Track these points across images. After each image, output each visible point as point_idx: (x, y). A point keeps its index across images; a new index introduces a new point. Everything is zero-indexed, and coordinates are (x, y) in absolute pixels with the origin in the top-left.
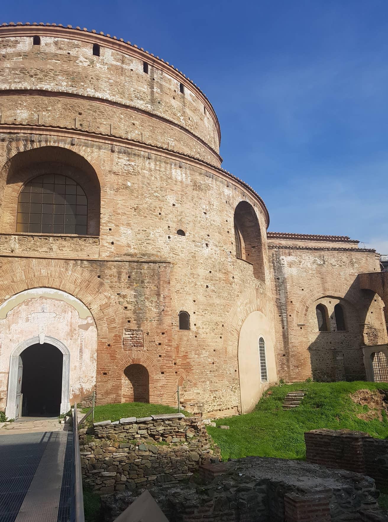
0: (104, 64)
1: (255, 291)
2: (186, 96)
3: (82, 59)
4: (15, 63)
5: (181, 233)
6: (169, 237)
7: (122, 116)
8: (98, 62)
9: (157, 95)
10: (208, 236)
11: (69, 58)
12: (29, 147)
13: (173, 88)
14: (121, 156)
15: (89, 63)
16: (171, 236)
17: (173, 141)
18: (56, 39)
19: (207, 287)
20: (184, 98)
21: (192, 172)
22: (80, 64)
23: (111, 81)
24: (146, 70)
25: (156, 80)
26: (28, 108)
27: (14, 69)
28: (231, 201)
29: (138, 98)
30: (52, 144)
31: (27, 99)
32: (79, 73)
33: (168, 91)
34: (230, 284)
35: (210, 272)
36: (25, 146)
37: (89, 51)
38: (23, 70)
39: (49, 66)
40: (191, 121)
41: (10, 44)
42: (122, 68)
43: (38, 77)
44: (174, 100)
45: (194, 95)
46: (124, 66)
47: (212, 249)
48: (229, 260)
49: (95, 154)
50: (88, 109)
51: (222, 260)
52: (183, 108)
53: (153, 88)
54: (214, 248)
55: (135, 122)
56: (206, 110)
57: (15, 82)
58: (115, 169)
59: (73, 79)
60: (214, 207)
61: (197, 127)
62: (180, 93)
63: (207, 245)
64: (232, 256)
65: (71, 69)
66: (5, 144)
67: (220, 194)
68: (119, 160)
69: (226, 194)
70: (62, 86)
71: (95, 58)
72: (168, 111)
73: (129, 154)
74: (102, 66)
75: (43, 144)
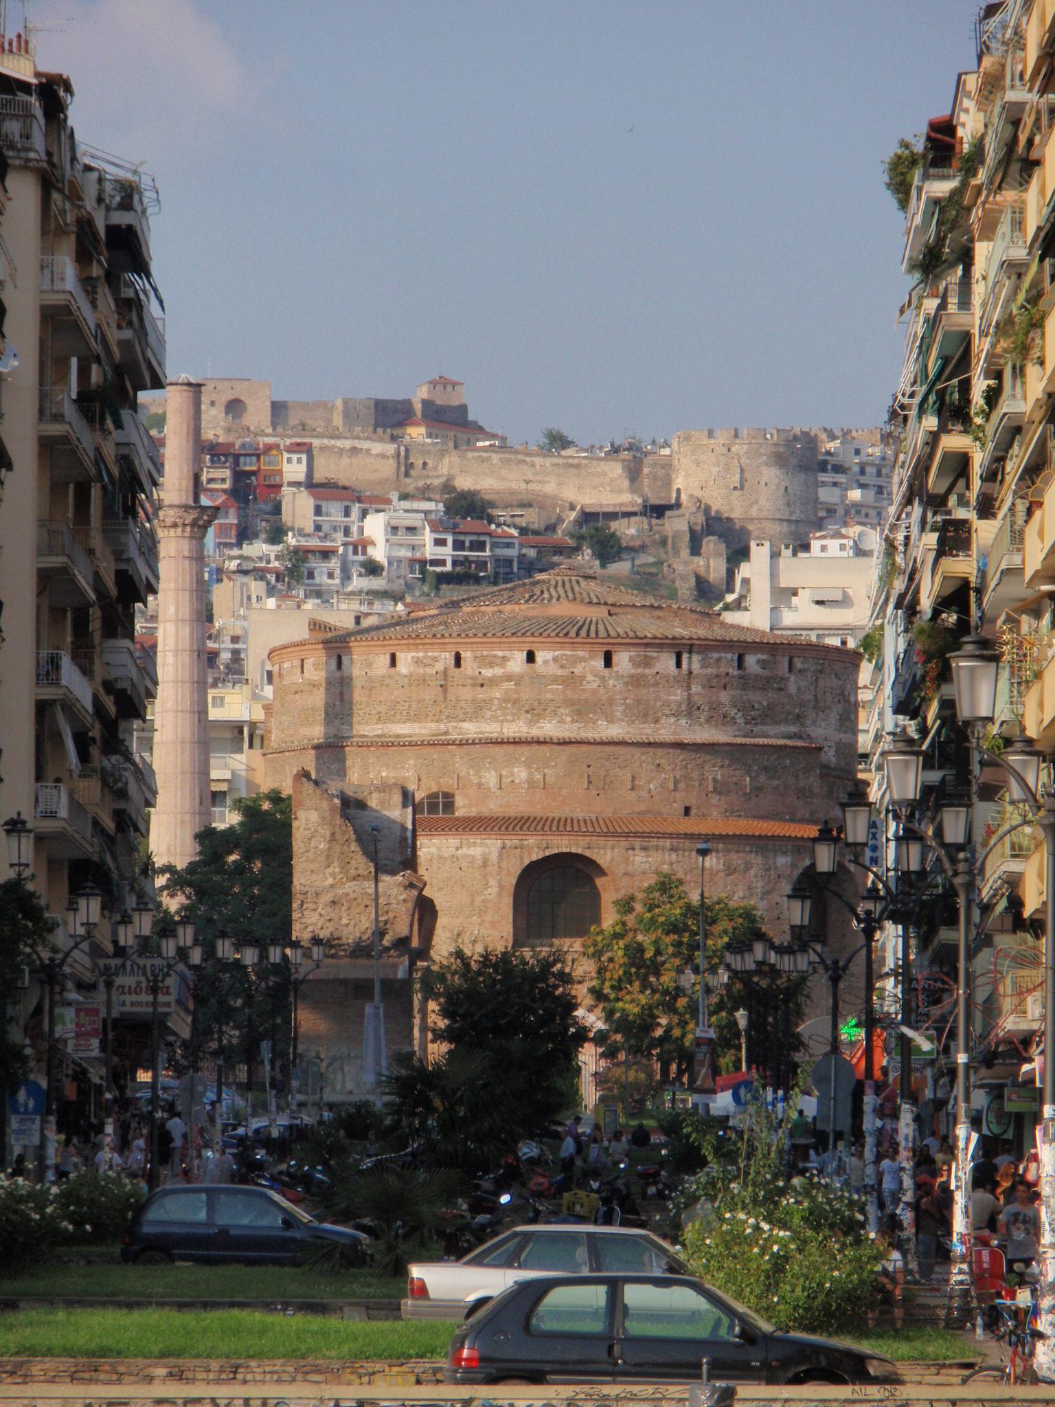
0: (619, 677)
2: (748, 671)
3: (590, 678)
4: (507, 691)
8: (610, 678)
9: (696, 698)
11: (572, 680)
12: (541, 856)
13: (723, 670)
14: (637, 852)
18: (557, 653)
22: (588, 686)
24: (679, 664)
26: (528, 765)
27: (505, 700)
29: (667, 716)
30: (565, 850)
31: (524, 749)
32: (586, 701)
37: (600, 663)
38: (515, 702)
39: (549, 696)
41: (498, 661)
45: (764, 657)
46: (647, 671)
53: (689, 688)
55: (662, 761)
56: (796, 660)
57: (508, 721)
58: (630, 868)
62: (736, 673)
66: (517, 851)
67: (768, 869)
71: (607, 672)
73: (644, 849)
75: (556, 851)
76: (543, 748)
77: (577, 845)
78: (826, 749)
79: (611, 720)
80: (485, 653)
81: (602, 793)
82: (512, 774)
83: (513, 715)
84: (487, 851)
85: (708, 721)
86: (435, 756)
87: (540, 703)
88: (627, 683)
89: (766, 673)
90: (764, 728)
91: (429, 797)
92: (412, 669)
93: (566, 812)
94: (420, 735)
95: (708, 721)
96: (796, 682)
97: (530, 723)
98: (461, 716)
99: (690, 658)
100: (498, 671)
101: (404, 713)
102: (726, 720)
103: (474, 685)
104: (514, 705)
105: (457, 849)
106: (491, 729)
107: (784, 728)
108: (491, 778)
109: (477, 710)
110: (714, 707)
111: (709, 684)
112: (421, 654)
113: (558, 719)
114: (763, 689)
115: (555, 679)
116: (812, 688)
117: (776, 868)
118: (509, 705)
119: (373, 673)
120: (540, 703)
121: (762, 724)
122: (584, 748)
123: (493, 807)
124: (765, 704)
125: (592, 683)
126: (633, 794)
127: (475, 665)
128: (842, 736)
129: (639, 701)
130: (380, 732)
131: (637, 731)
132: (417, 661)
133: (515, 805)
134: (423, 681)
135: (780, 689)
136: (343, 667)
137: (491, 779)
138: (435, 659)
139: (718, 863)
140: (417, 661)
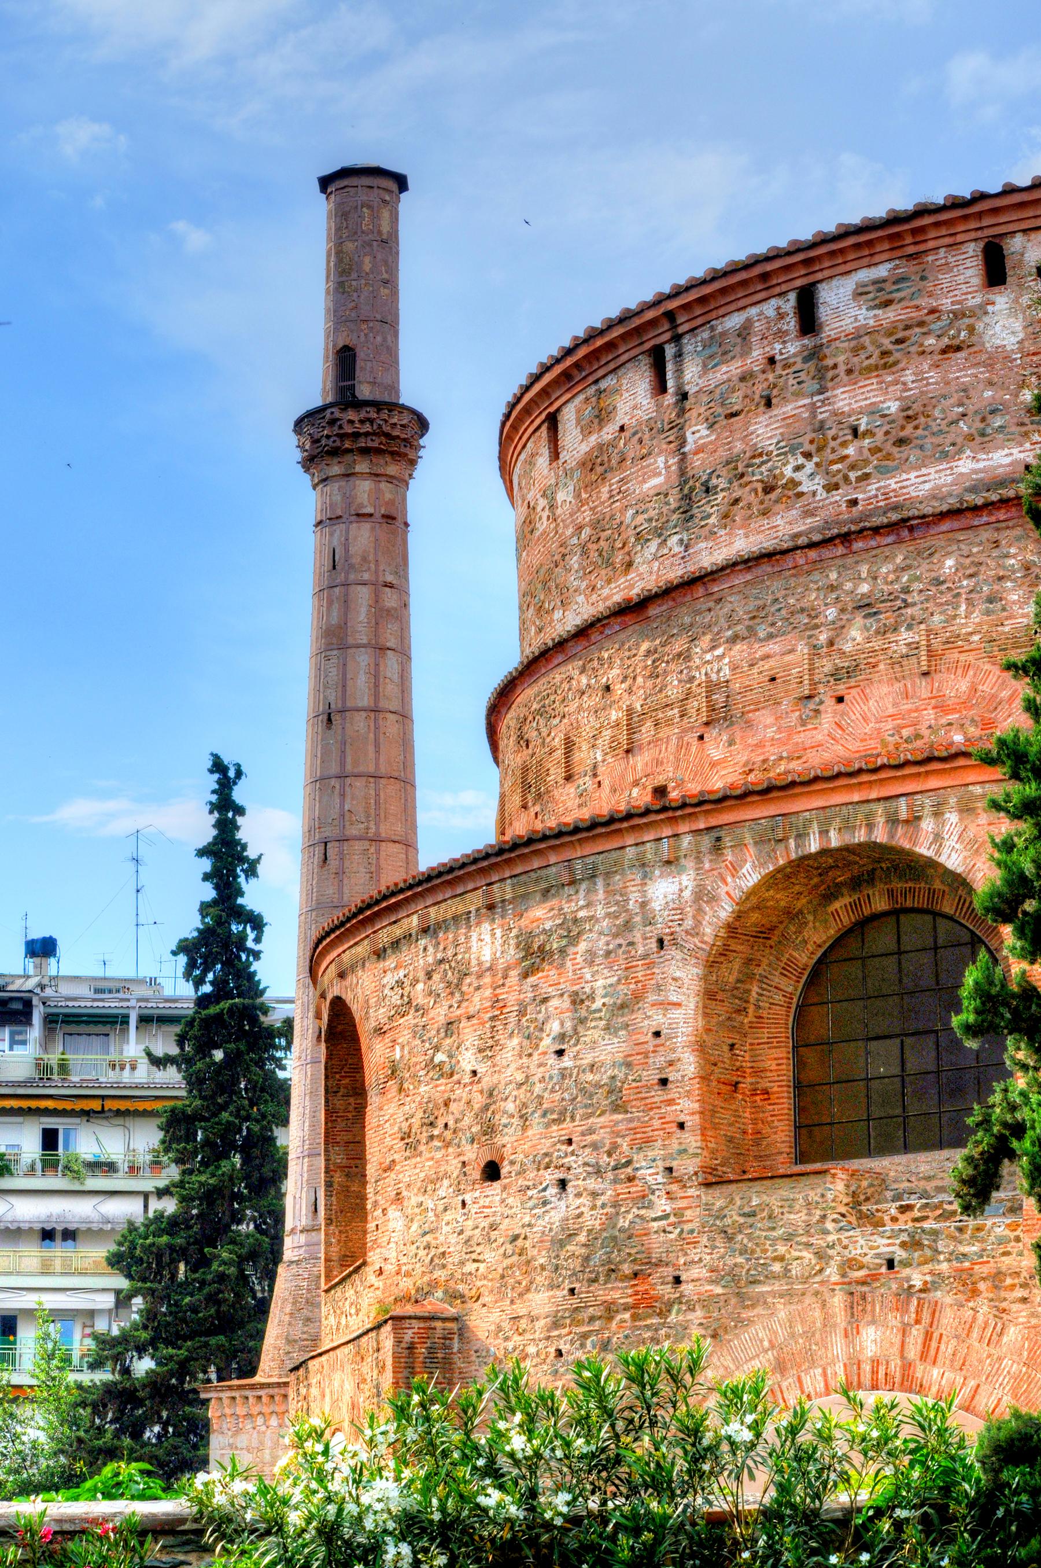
1: (838, 1301)
5: (492, 1172)
6: (464, 1204)
7: (584, 680)
9: (697, 464)
10: (570, 1142)
13: (757, 354)
16: (468, 1198)
17: (723, 656)
19: (559, 1353)
20: (814, 354)
24: (660, 387)
25: (692, 389)
28: (689, 923)
33: (736, 401)
34: (660, 1314)
35: (572, 1291)
37: (543, 461)
40: (869, 433)
45: (882, 271)
47: (579, 1195)
48: (662, 1205)
51: (621, 1224)
52: (814, 414)
53: (683, 443)
54: (592, 1184)
56: (1015, 244)
60: (594, 1006)
61: (908, 431)
62: (793, 348)
63: (563, 1184)
64: (674, 1187)
67: (628, 926)
69: (656, 905)
72: (736, 501)
89: (890, 315)
90: (892, 483)
107: (965, 465)
114: (886, 363)
121: (884, 471)
124: (893, 407)
135: (958, 349)
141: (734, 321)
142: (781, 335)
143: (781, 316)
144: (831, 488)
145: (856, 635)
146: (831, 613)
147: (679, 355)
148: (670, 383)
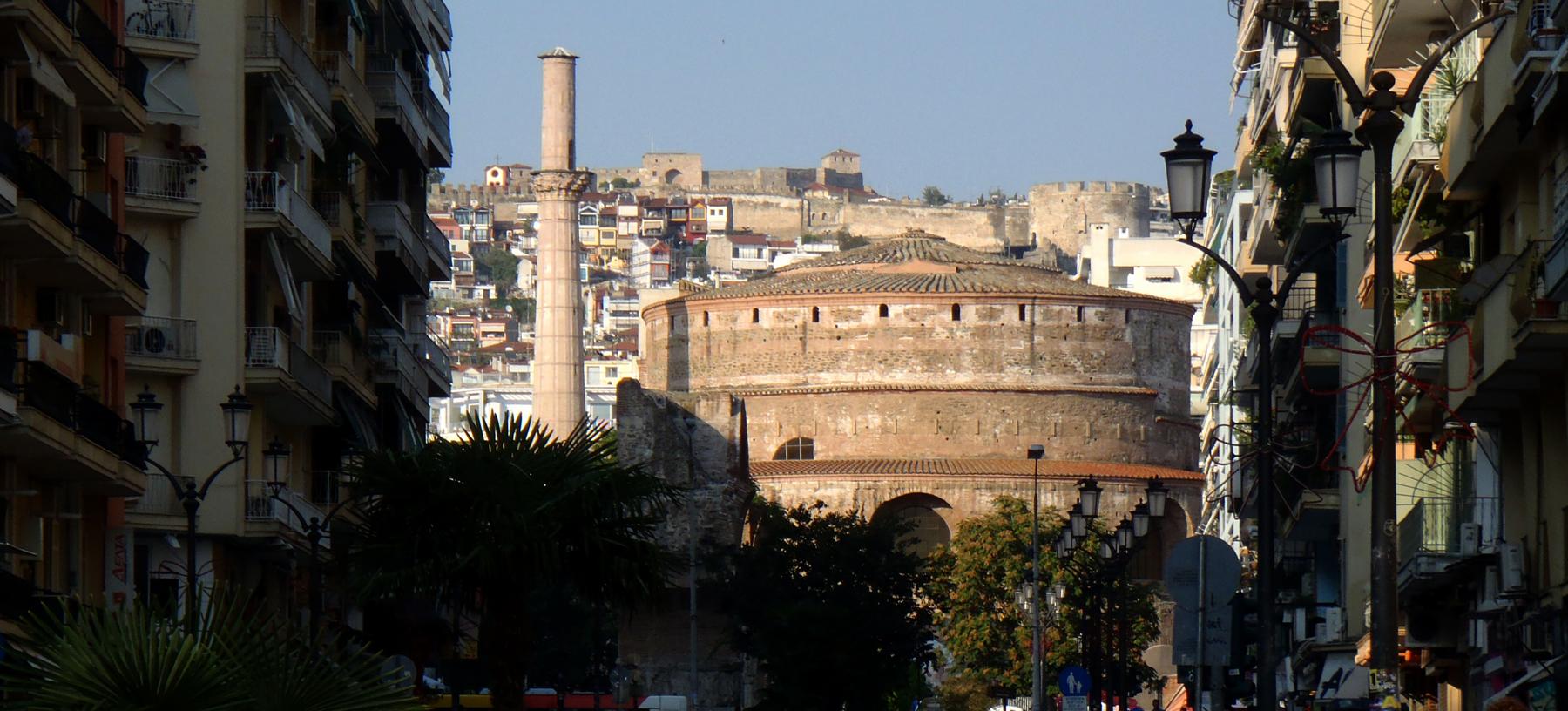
0: (966, 329)
2: (1087, 323)
3: (939, 329)
4: (862, 342)
8: (957, 330)
9: (1038, 348)
11: (922, 332)
13: (1063, 322)
15: (947, 334)
18: (908, 307)
21: (1067, 492)
22: (937, 338)
23: (974, 351)
24: (1022, 317)
25: (1037, 323)
26: (881, 411)
27: (860, 352)
29: (1011, 365)
30: (915, 491)
31: (878, 397)
32: (936, 352)
36: (890, 494)
37: (948, 316)
39: (901, 347)
41: (853, 315)
42: (990, 327)
43: (888, 362)
44: (1065, 343)
45: (1103, 309)
46: (993, 323)
49: (957, 495)
50: (947, 405)
55: (1007, 407)
56: (1132, 312)
57: (862, 371)
59: (928, 361)
62: (1076, 324)
65: (927, 347)
68: (983, 497)
69: (1116, 503)
70: (915, 372)
71: (954, 324)
74: (963, 334)
75: (907, 492)
76: (896, 395)
77: (927, 486)
78: (1161, 396)
79: (958, 369)
80: (841, 308)
81: (950, 437)
82: (867, 421)
83: (867, 365)
84: (843, 491)
85: (1049, 370)
86: (795, 405)
87: (892, 354)
88: (973, 335)
89: (1104, 324)
90: (1103, 376)
91: (790, 442)
92: (773, 323)
93: (917, 454)
94: (780, 385)
95: (1049, 370)
96: (1132, 333)
97: (882, 372)
98: (819, 367)
99: (1033, 311)
100: (853, 324)
101: (766, 365)
102: (1067, 368)
103: (831, 338)
104: (870, 357)
105: (816, 490)
106: (847, 378)
108: (846, 425)
109: (834, 361)
110: (1056, 356)
111: (1050, 335)
112: (781, 310)
113: (908, 368)
115: (906, 331)
116: (1148, 338)
117: (1114, 506)
118: (864, 356)
119: (738, 328)
120: (892, 354)
121: (1100, 372)
122: (935, 395)
123: (849, 451)
124: (1103, 353)
125: (941, 334)
126: (980, 439)
127: (832, 319)
128: (1176, 384)
129: (984, 352)
130: (744, 383)
131: (984, 380)
132: (778, 316)
133: (870, 448)
134: (784, 334)
136: (709, 322)
137: (846, 425)
138: (795, 314)
139: (1059, 502)
140: (778, 316)
141: (1056, 308)
142: (1071, 318)
143: (1073, 312)
144: (1085, 372)
145: (1101, 421)
146: (1094, 413)
147: (1033, 311)
148: (1027, 317)
